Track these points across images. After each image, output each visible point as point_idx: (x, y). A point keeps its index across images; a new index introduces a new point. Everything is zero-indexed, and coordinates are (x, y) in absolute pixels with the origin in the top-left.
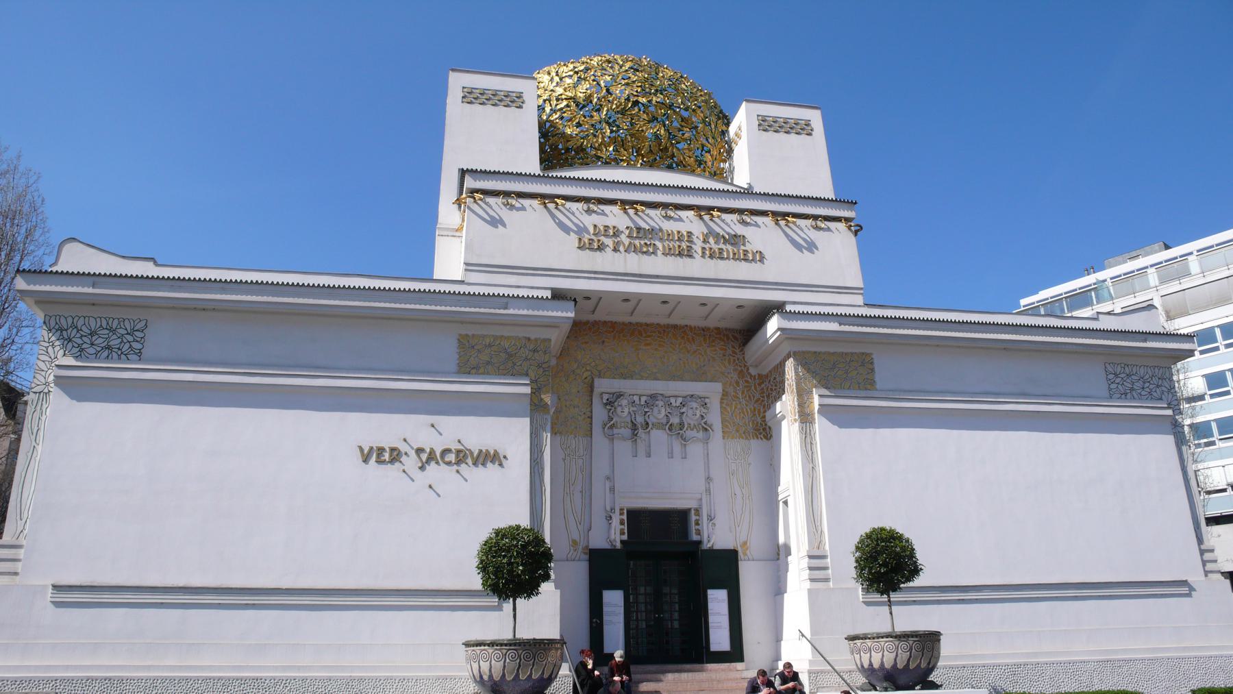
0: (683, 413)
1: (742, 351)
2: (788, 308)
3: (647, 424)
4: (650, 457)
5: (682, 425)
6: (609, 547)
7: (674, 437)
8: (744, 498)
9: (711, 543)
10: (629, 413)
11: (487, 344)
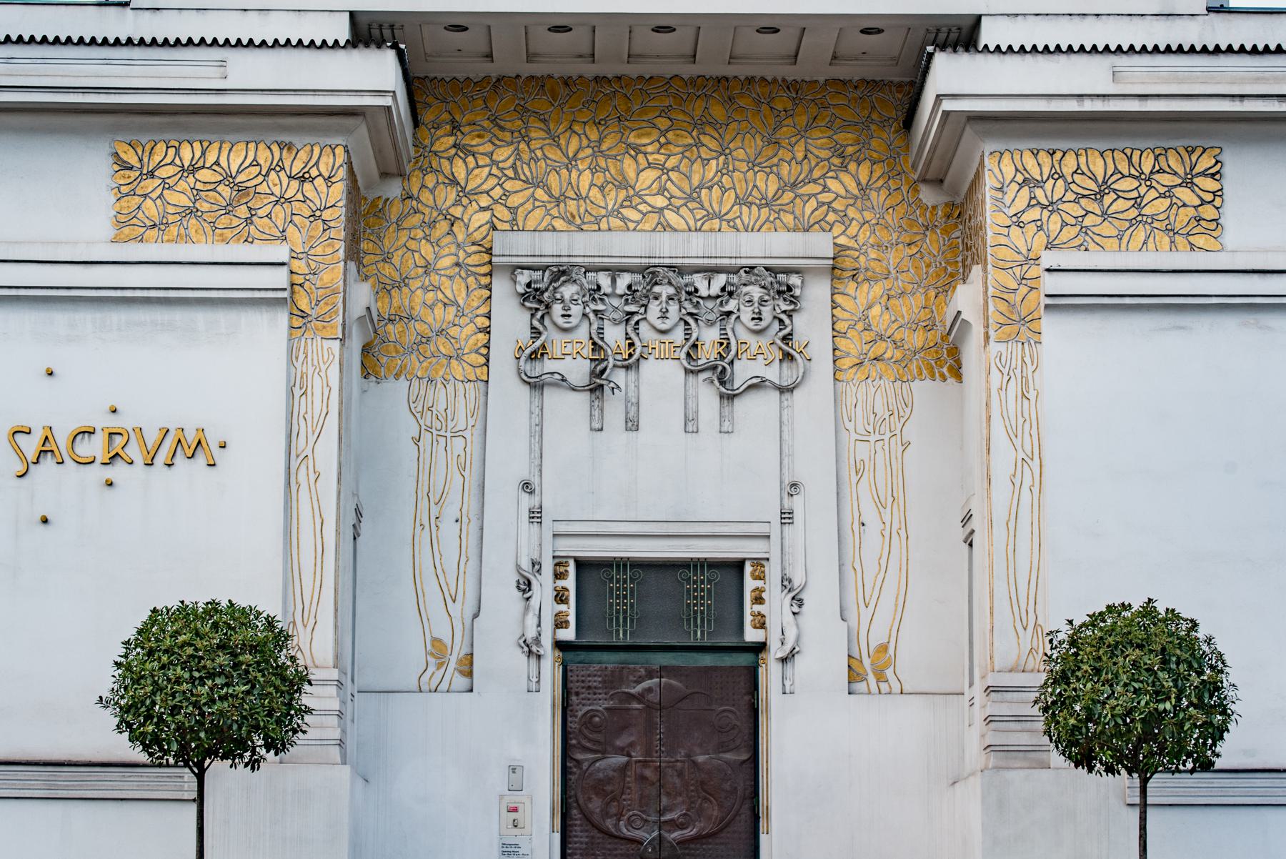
2: (989, 35)
3: (631, 345)
4: (636, 427)
5: (725, 344)
8: (887, 533)
9: (788, 648)
10: (585, 315)
11: (186, 164)
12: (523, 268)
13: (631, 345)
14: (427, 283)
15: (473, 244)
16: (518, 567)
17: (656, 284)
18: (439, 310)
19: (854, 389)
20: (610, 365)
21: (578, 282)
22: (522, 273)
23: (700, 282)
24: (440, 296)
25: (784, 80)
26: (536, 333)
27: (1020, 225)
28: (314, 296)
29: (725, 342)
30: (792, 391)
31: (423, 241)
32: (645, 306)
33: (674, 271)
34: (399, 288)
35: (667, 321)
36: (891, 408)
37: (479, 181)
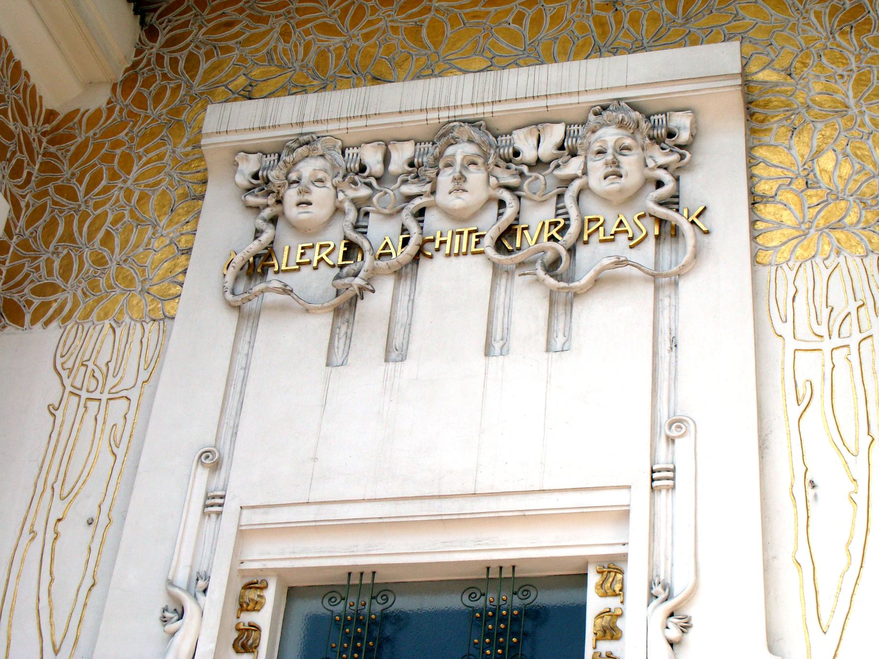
0: (576, 177)
10: (338, 210)
13: (405, 242)
19: (791, 275)
21: (328, 157)
22: (247, 160)
30: (676, 284)
32: (433, 182)
35: (464, 195)
36: (859, 295)
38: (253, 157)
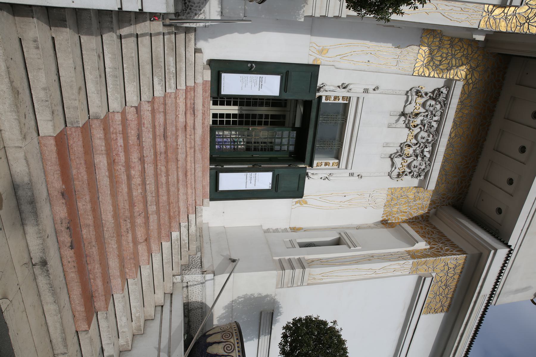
0: (417, 159)
1: (449, 204)
3: (415, 126)
6: (319, 83)
7: (399, 148)
8: (341, 203)
12: (448, 92)
14: (449, 54)
15: (457, 72)
16: (351, 84)
17: (433, 136)
18: (439, 58)
20: (411, 119)
23: (429, 148)
24: (444, 59)
25: (474, 171)
26: (426, 94)
27: (444, 266)
28: (498, 17)
29: (408, 156)
30: (389, 175)
31: (462, 54)
33: (435, 141)
34: (449, 44)
35: (420, 139)
37: (475, 75)
38: (446, 92)
